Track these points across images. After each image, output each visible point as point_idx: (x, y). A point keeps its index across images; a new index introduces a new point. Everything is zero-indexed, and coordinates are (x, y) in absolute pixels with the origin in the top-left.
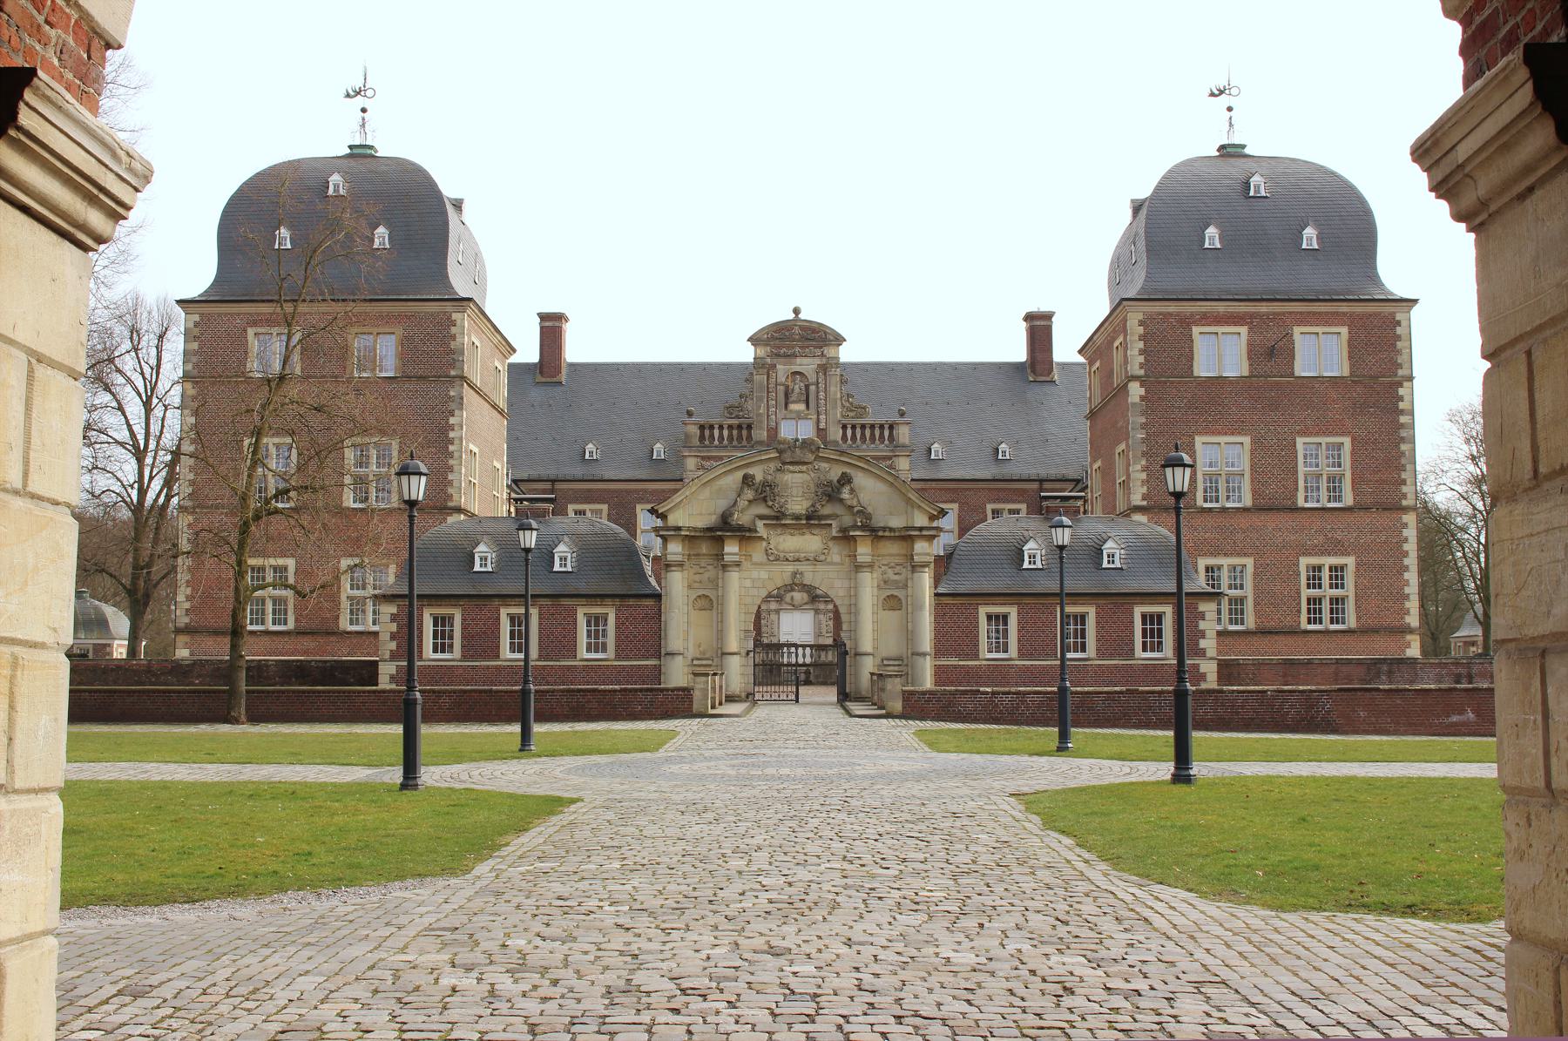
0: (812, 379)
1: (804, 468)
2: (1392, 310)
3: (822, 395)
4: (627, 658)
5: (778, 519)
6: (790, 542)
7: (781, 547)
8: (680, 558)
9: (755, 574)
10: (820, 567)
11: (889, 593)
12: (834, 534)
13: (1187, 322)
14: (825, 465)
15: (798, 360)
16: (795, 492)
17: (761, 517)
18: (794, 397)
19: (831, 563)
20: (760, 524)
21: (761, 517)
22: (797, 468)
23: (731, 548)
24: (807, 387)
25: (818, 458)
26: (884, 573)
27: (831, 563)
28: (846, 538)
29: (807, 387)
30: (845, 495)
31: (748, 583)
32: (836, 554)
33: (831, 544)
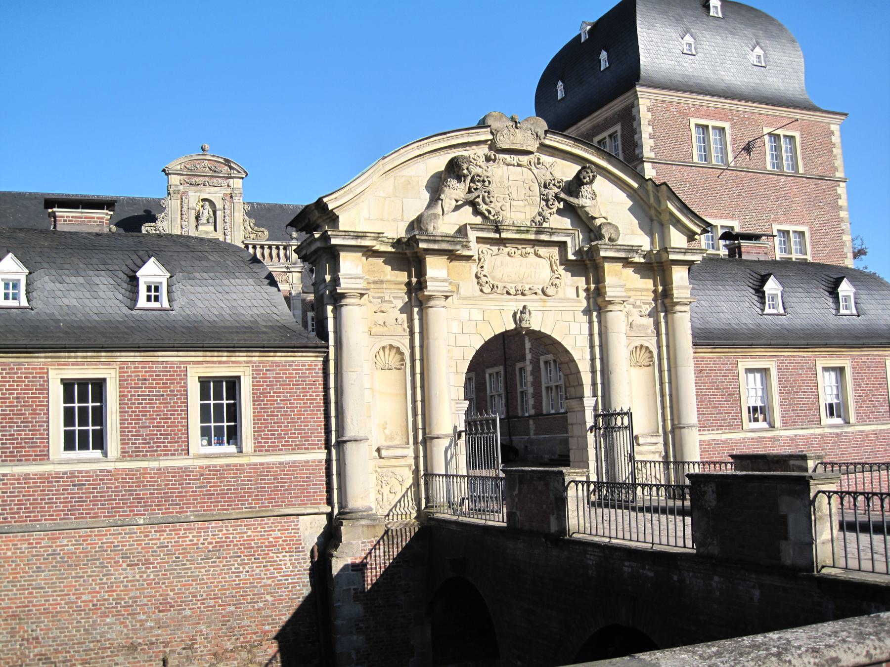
0: (219, 205)
1: (524, 159)
2: (827, 120)
3: (227, 219)
4: (273, 449)
5: (497, 236)
6: (506, 266)
7: (498, 274)
8: (362, 285)
9: (464, 314)
10: (550, 304)
11: (638, 343)
12: (571, 257)
13: (684, 114)
14: (546, 159)
15: (207, 189)
16: (514, 196)
17: (475, 227)
18: (203, 220)
19: (565, 300)
20: (472, 235)
21: (475, 227)
22: (515, 159)
23: (436, 269)
24: (215, 213)
25: (545, 148)
26: (628, 314)
27: (565, 300)
28: (587, 265)
29: (215, 213)
30: (584, 201)
31: (455, 327)
32: (573, 286)
33: (561, 269)
